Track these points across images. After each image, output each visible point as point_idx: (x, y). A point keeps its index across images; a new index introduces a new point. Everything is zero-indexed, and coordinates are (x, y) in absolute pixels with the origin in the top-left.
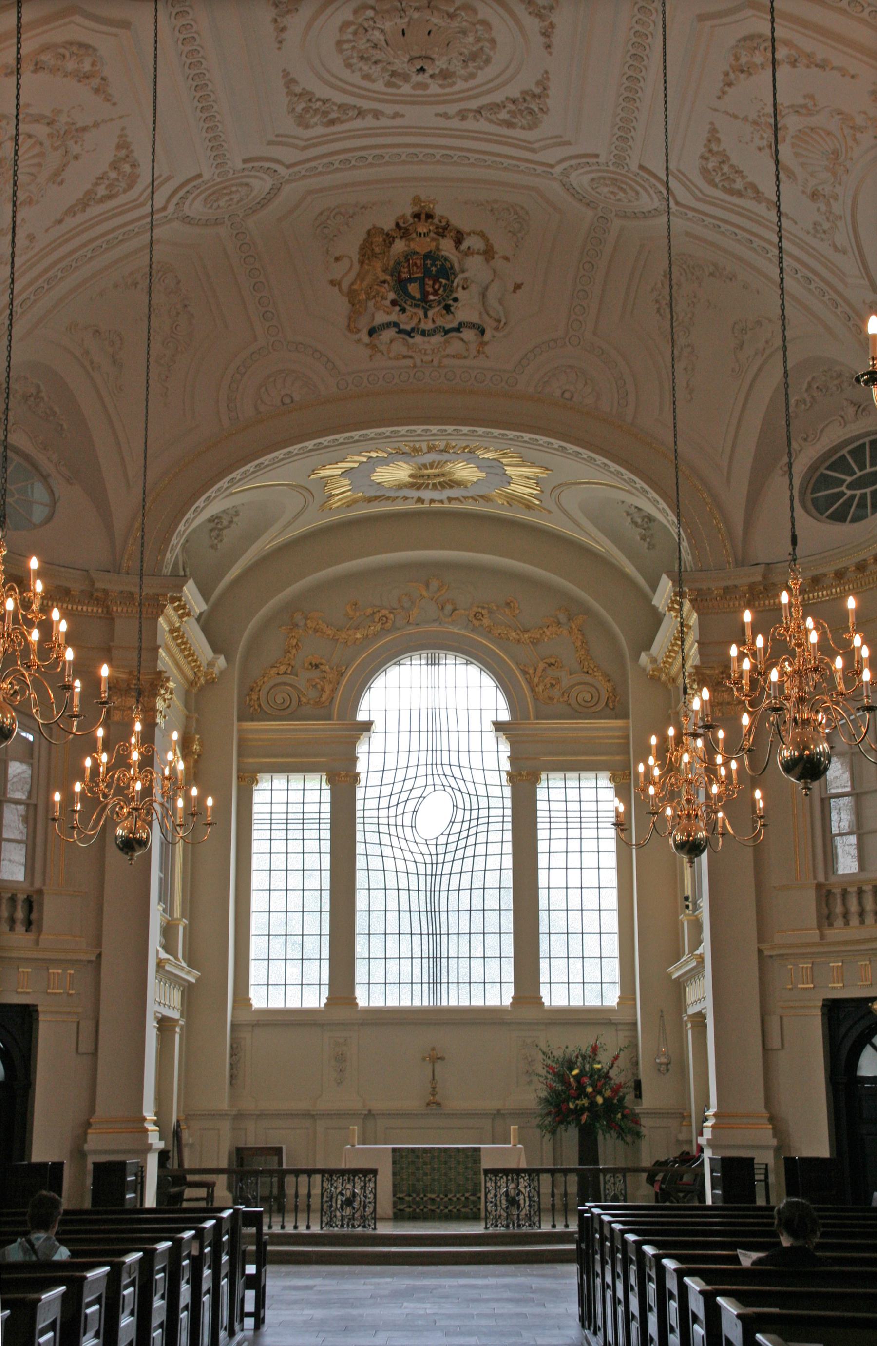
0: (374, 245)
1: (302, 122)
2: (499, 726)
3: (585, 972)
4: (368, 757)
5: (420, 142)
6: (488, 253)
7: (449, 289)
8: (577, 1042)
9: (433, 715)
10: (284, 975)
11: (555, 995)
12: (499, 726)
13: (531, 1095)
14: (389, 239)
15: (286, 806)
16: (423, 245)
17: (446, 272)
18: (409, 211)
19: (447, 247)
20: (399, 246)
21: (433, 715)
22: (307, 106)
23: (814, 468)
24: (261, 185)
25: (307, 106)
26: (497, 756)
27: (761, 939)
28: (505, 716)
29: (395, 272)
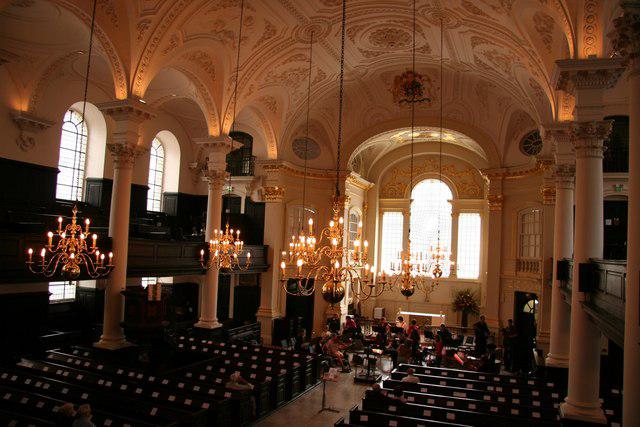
0: (398, 80)
1: (367, 56)
2: (448, 201)
3: (470, 267)
4: (414, 208)
5: (399, 58)
6: (429, 80)
7: (420, 90)
8: (463, 288)
9: (432, 196)
10: (388, 263)
11: (461, 275)
12: (448, 201)
13: (450, 300)
14: (401, 78)
15: (392, 221)
16: (411, 80)
17: (419, 86)
18: (405, 71)
19: (417, 79)
20: (405, 80)
21: (432, 196)
22: (367, 54)
23: (524, 137)
24: (364, 71)
25: (367, 54)
26: (449, 207)
27: (501, 273)
28: (451, 197)
29: (404, 86)
